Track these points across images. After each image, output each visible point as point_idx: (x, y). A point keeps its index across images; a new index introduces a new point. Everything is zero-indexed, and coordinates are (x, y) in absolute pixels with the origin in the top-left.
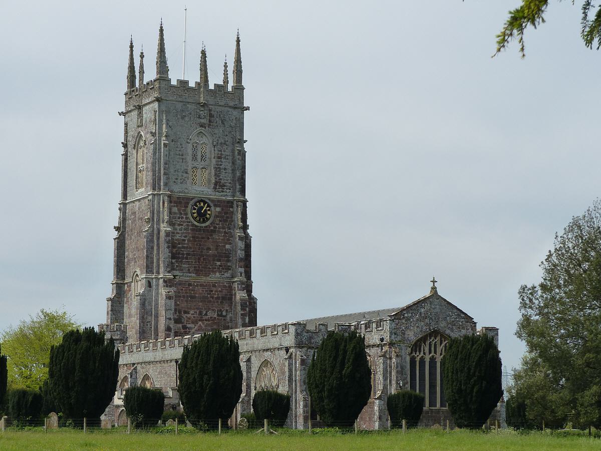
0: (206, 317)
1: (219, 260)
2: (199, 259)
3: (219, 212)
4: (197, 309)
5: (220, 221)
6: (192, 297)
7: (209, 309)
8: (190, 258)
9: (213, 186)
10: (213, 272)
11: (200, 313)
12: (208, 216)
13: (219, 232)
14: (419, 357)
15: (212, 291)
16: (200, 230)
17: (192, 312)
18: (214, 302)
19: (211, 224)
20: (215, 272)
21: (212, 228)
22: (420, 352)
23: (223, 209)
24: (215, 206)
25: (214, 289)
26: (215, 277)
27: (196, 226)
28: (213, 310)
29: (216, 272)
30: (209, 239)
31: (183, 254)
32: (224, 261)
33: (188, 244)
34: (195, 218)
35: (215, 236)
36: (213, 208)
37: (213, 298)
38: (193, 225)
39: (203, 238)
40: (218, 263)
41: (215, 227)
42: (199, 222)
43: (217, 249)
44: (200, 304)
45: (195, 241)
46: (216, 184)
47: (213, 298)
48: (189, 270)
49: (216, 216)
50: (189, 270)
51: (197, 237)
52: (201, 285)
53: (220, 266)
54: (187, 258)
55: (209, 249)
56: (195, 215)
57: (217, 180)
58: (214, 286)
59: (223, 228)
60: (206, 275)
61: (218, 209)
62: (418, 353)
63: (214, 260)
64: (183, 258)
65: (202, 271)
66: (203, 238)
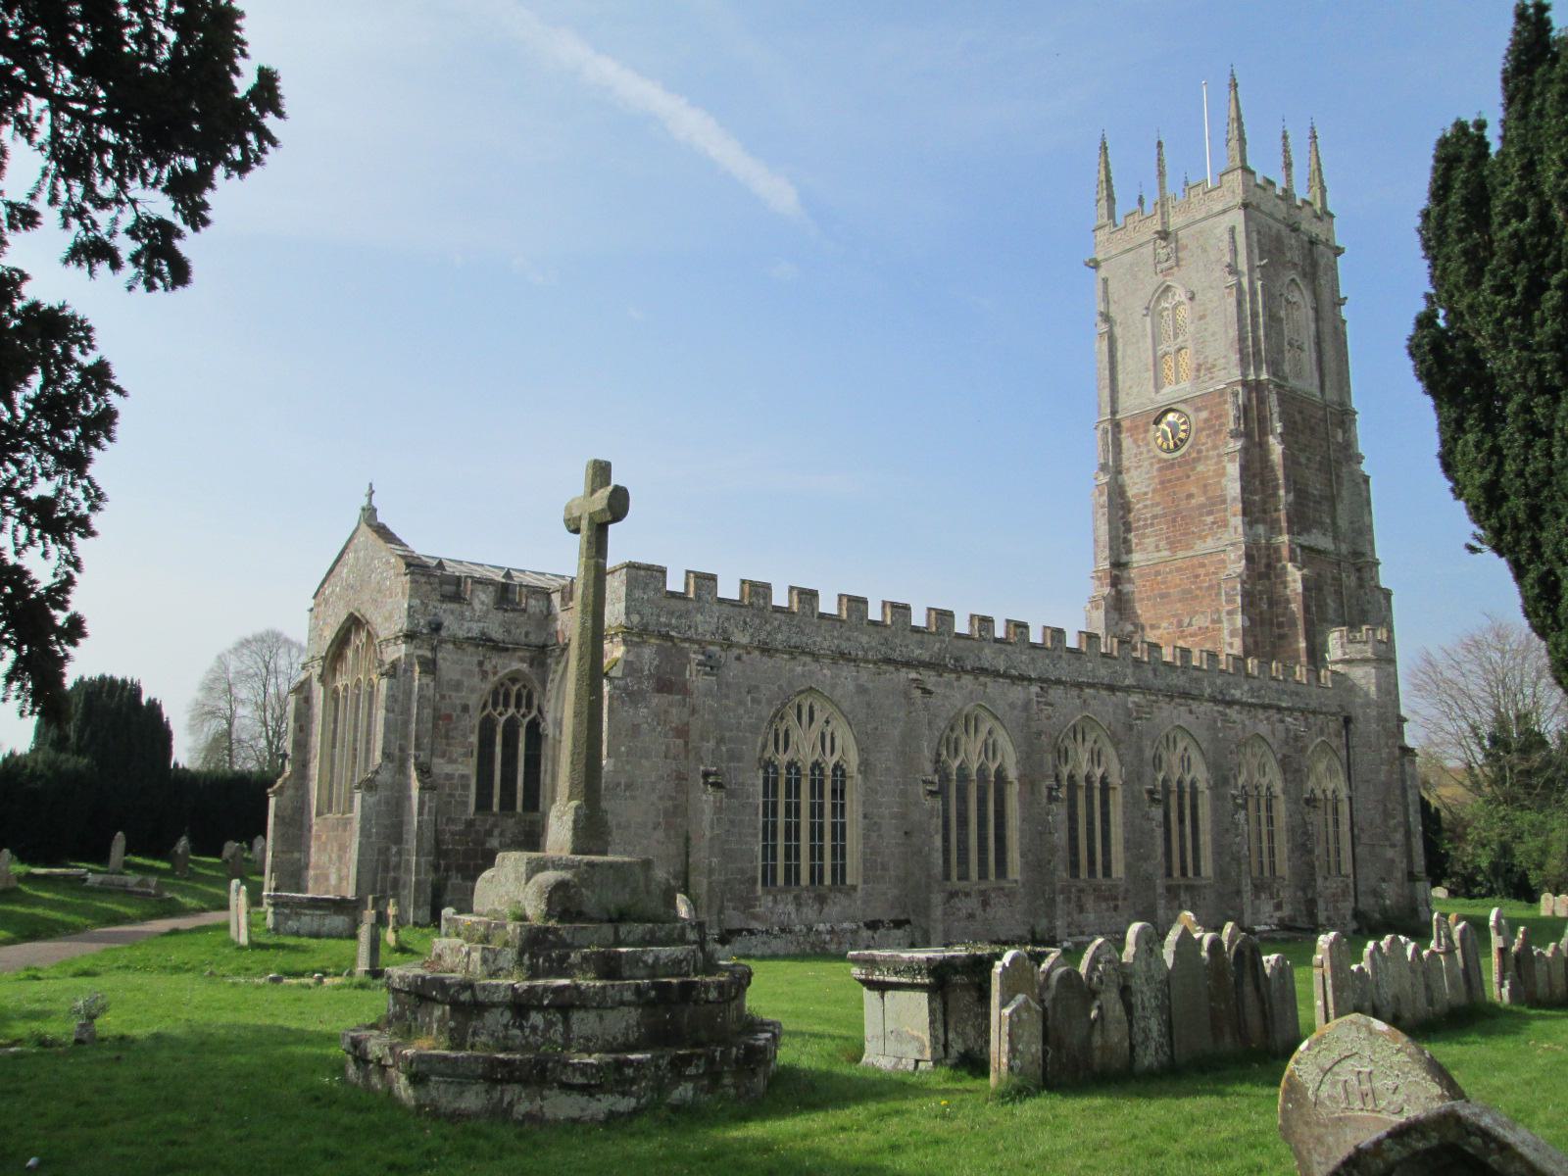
0: (1192, 629)
1: (1210, 513)
2: (1174, 520)
3: (1206, 421)
4: (1174, 616)
5: (1208, 436)
6: (1163, 596)
7: (1196, 612)
8: (1159, 524)
9: (1194, 374)
10: (1200, 538)
11: (1180, 624)
12: (1182, 435)
13: (1207, 458)
14: (504, 718)
15: (1197, 576)
16: (1173, 465)
17: (1164, 625)
18: (1204, 597)
19: (1191, 446)
20: (1203, 538)
21: (1194, 455)
22: (506, 705)
23: (1212, 412)
24: (1198, 410)
25: (1202, 571)
26: (1210, 544)
27: (1166, 461)
28: (1203, 613)
29: (1206, 536)
30: (1188, 477)
31: (1146, 519)
32: (1219, 511)
33: (1152, 499)
34: (1161, 447)
35: (1200, 468)
36: (1192, 418)
37: (1200, 588)
38: (1160, 460)
39: (1178, 479)
40: (1210, 519)
41: (1199, 452)
42: (1169, 451)
43: (1205, 492)
44: (1179, 605)
45: (1164, 489)
46: (1200, 365)
47: (1200, 588)
48: (1157, 546)
49: (1199, 431)
50: (1157, 546)
51: (1170, 481)
52: (1179, 569)
53: (1213, 523)
54: (1152, 525)
55: (1190, 496)
56: (1160, 441)
57: (1201, 361)
58: (1203, 565)
59: (1215, 447)
60: (1189, 547)
61: (1204, 414)
62: (523, 710)
63: (1201, 515)
64: (1145, 526)
65: (1180, 541)
66: (1178, 479)
